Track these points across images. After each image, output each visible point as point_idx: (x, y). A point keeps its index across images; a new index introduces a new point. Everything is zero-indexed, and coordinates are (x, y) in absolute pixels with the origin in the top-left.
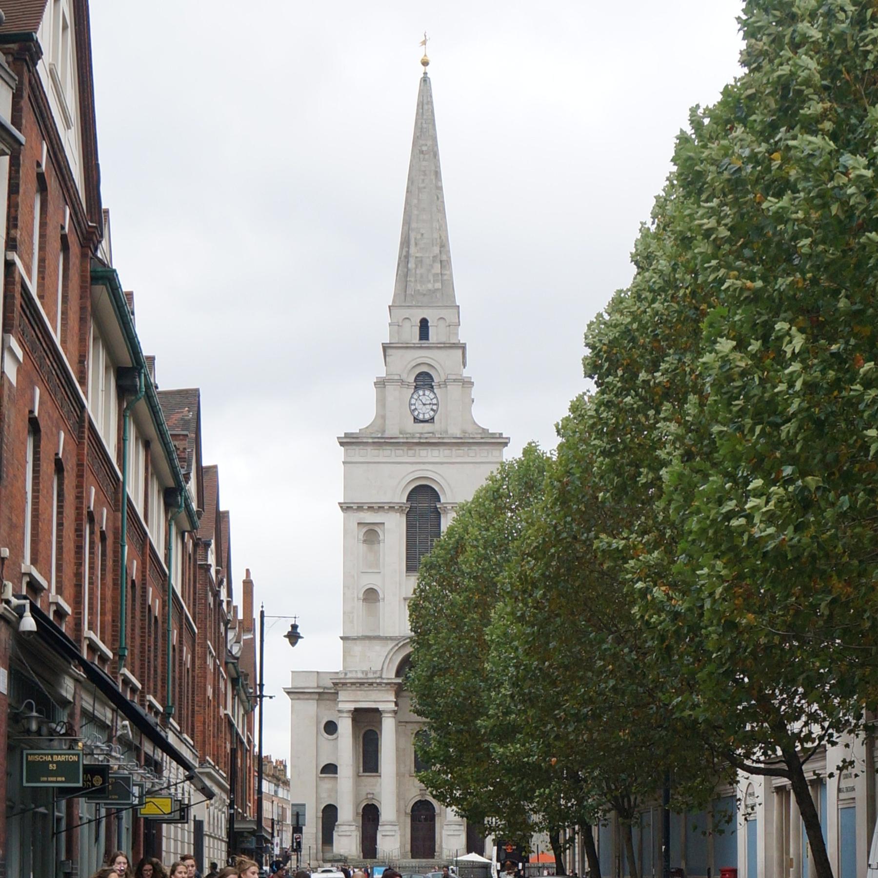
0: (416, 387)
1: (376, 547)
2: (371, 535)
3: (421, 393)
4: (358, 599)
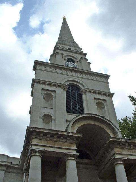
0: (67, 61)
1: (49, 102)
2: (48, 96)
3: (70, 62)
4: (40, 117)
